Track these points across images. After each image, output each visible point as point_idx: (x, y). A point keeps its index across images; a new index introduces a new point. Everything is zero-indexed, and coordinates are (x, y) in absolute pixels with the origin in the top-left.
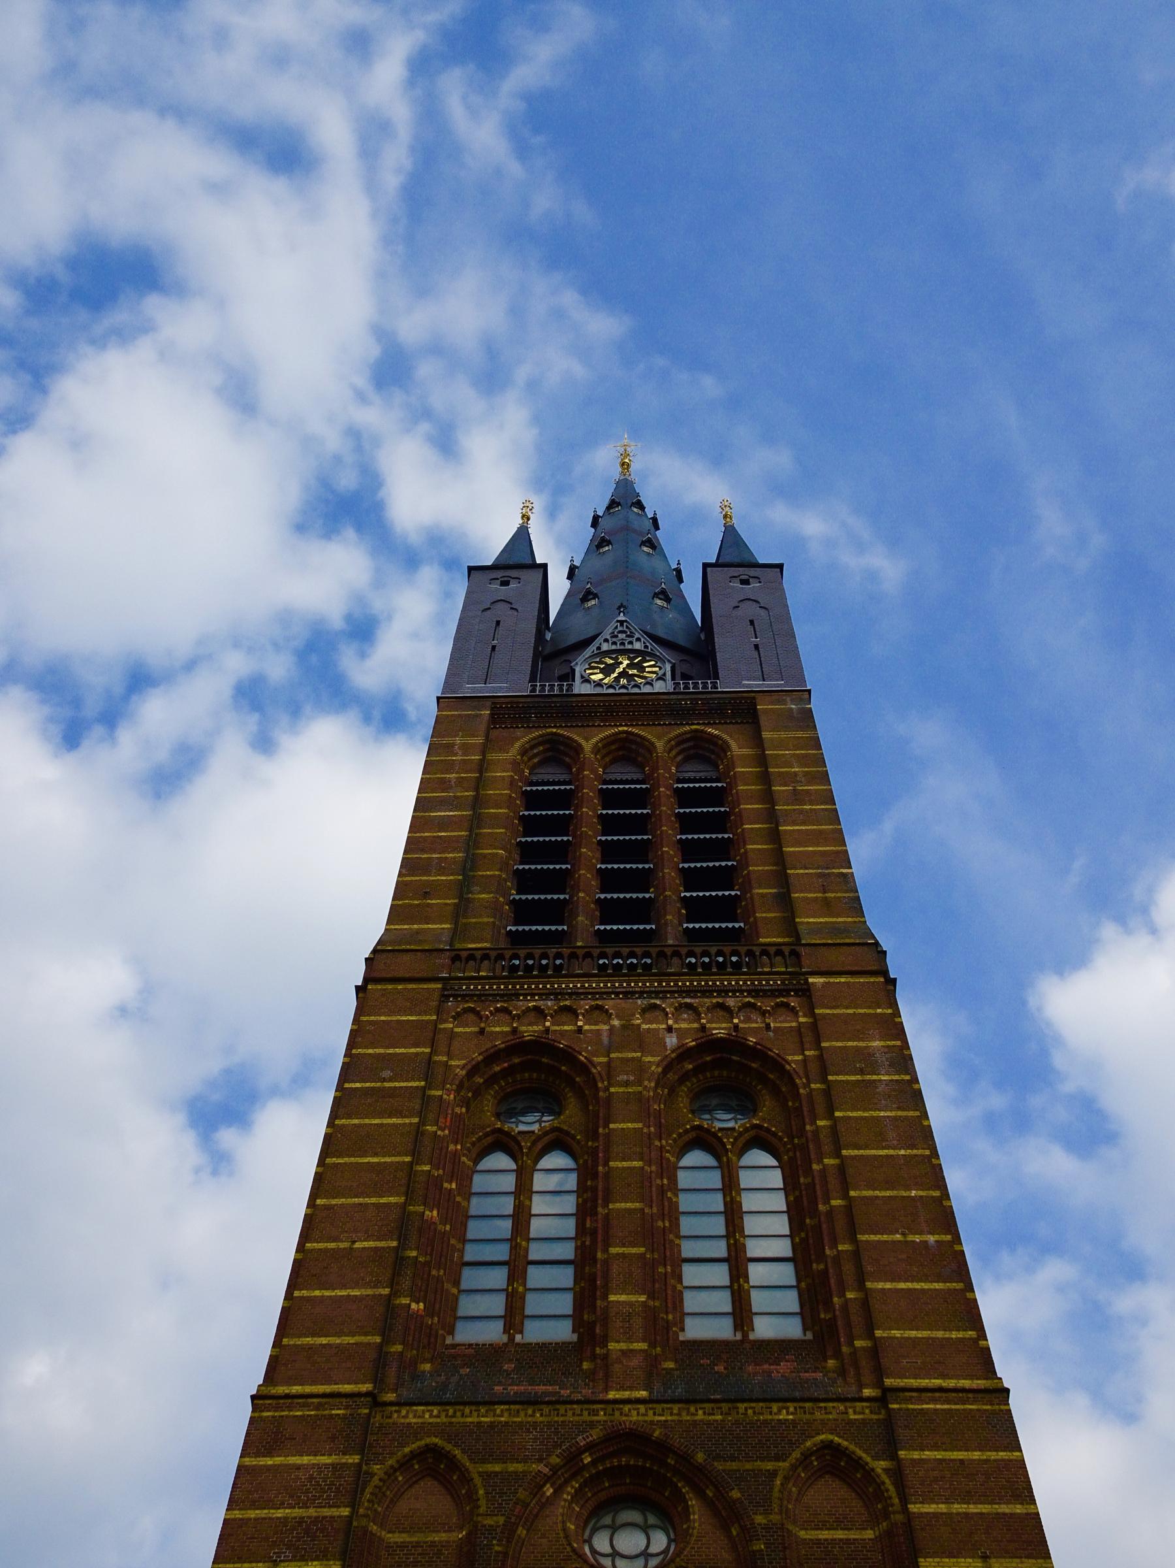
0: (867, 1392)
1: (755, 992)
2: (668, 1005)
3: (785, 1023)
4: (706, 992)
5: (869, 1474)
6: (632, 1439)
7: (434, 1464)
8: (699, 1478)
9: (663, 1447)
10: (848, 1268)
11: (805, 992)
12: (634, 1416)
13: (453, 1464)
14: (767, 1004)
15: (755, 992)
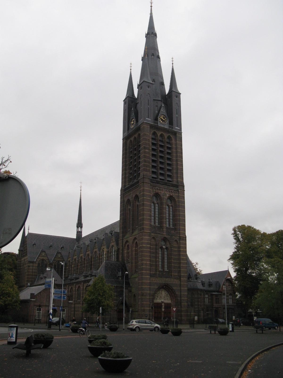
0: (179, 236)
1: (175, 190)
2: (168, 190)
3: (176, 194)
4: (171, 189)
5: (178, 242)
6: (165, 237)
7: (153, 238)
8: (168, 241)
9: (167, 238)
10: (179, 224)
11: (178, 191)
12: (165, 236)
13: (155, 238)
14: (175, 192)
15: (175, 190)
